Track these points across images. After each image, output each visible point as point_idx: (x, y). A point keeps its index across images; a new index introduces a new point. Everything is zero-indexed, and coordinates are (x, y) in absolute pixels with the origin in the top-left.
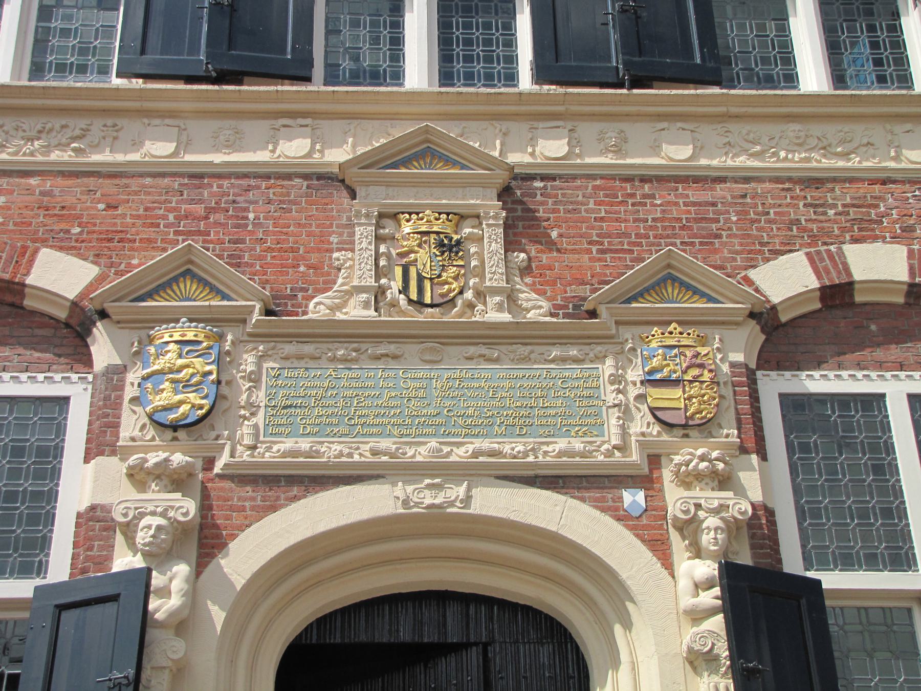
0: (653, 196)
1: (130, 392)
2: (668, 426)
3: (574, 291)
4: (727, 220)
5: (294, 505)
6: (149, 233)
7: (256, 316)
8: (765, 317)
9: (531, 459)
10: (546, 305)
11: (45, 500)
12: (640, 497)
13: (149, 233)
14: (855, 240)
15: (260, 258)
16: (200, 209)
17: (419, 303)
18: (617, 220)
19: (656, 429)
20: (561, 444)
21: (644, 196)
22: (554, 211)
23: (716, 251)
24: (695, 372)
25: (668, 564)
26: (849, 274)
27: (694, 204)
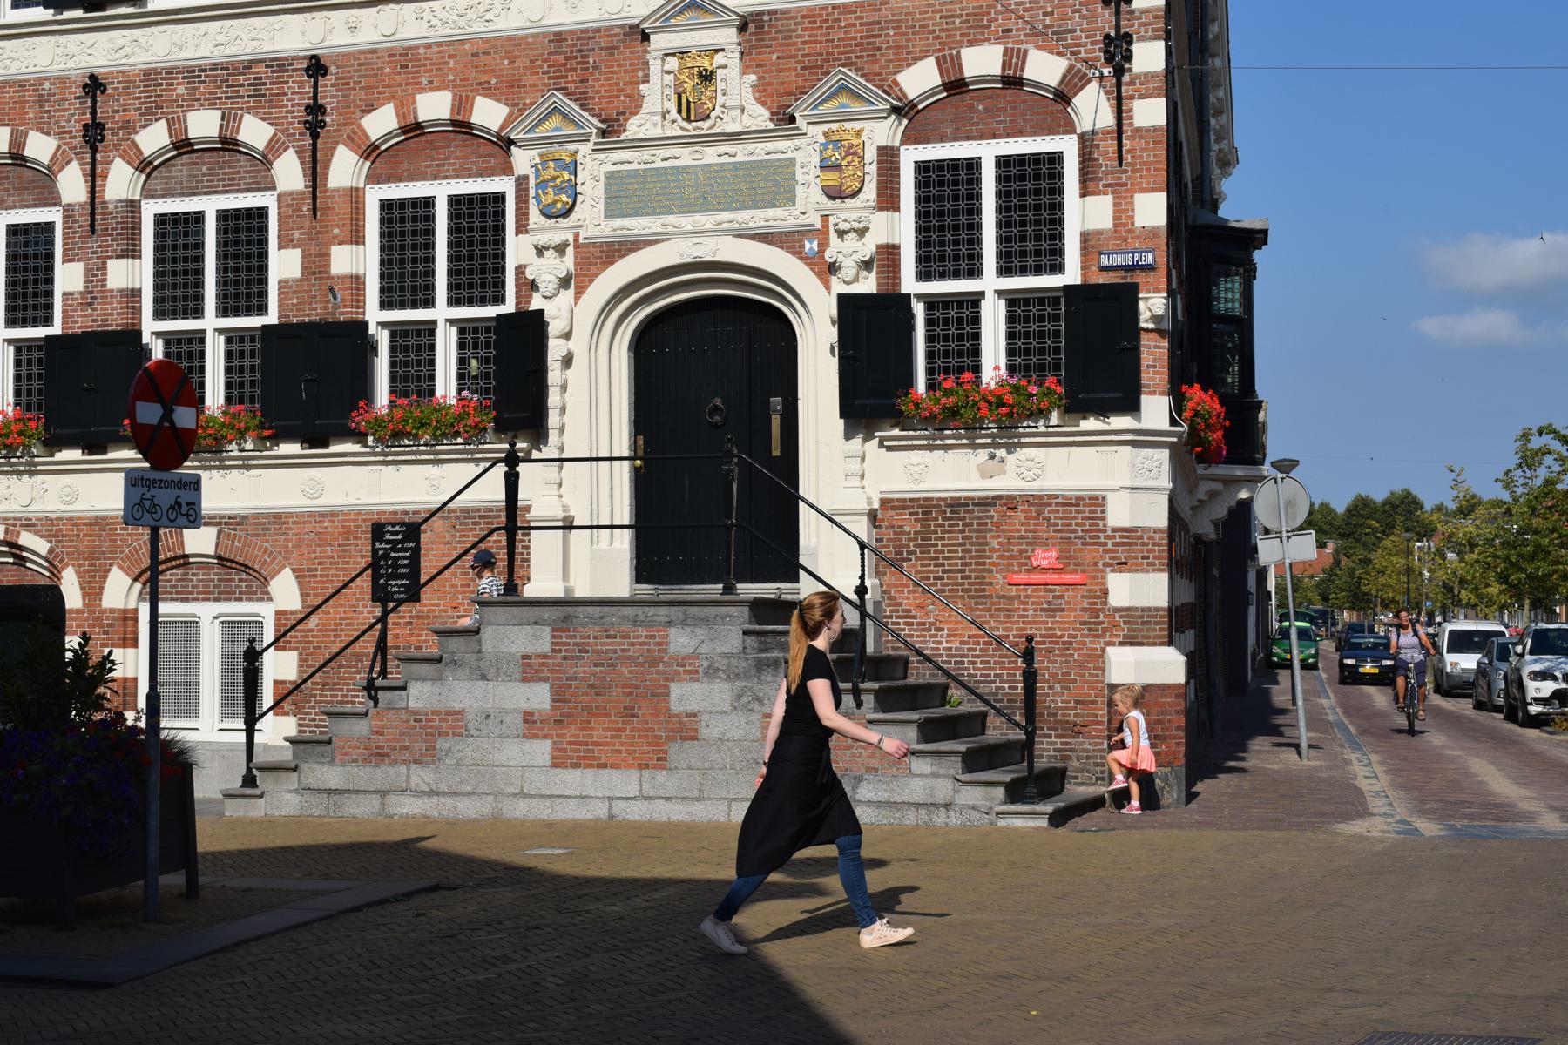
0: (839, 20)
1: (532, 192)
2: (832, 198)
3: (783, 101)
4: (887, 35)
5: (624, 260)
6: (533, 80)
7: (593, 139)
8: (904, 109)
9: (751, 225)
10: (767, 114)
11: (500, 256)
12: (815, 245)
13: (533, 80)
14: (971, 43)
15: (598, 92)
16: (561, 58)
17: (688, 120)
18: (816, 42)
19: (825, 199)
20: (771, 213)
21: (835, 21)
22: (775, 39)
23: (877, 61)
24: (849, 158)
25: (828, 288)
26: (961, 71)
27: (866, 24)
